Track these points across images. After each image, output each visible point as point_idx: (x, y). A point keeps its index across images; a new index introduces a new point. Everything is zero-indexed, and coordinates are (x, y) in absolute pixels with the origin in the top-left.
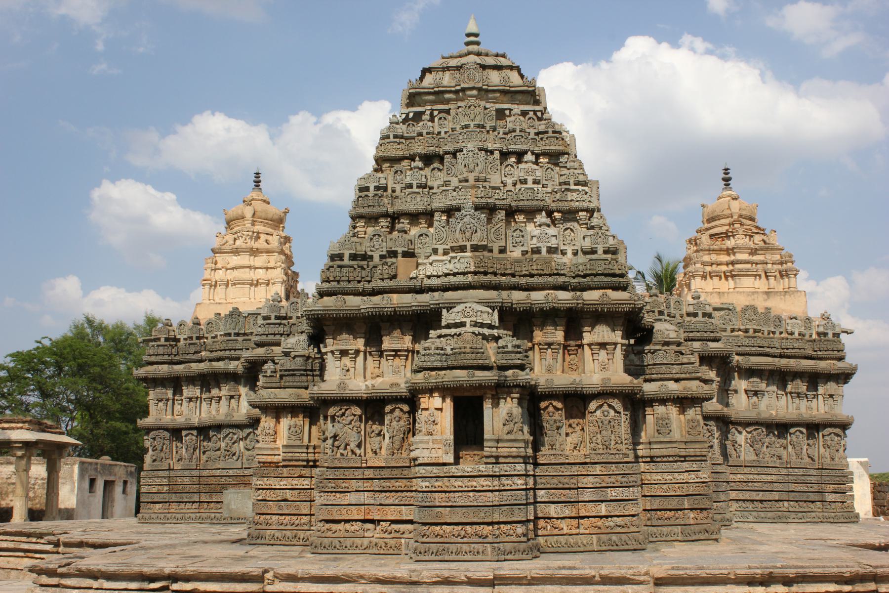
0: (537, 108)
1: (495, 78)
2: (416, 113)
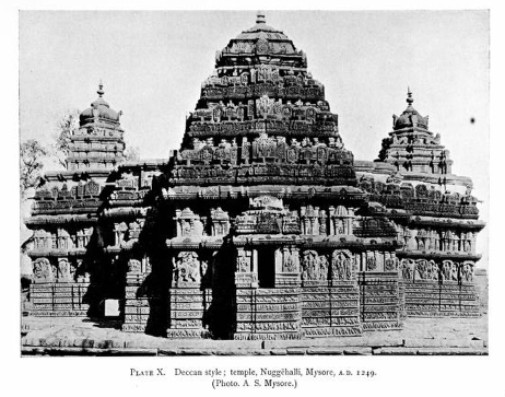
0: (303, 69)
1: (277, 48)
2: (228, 70)
